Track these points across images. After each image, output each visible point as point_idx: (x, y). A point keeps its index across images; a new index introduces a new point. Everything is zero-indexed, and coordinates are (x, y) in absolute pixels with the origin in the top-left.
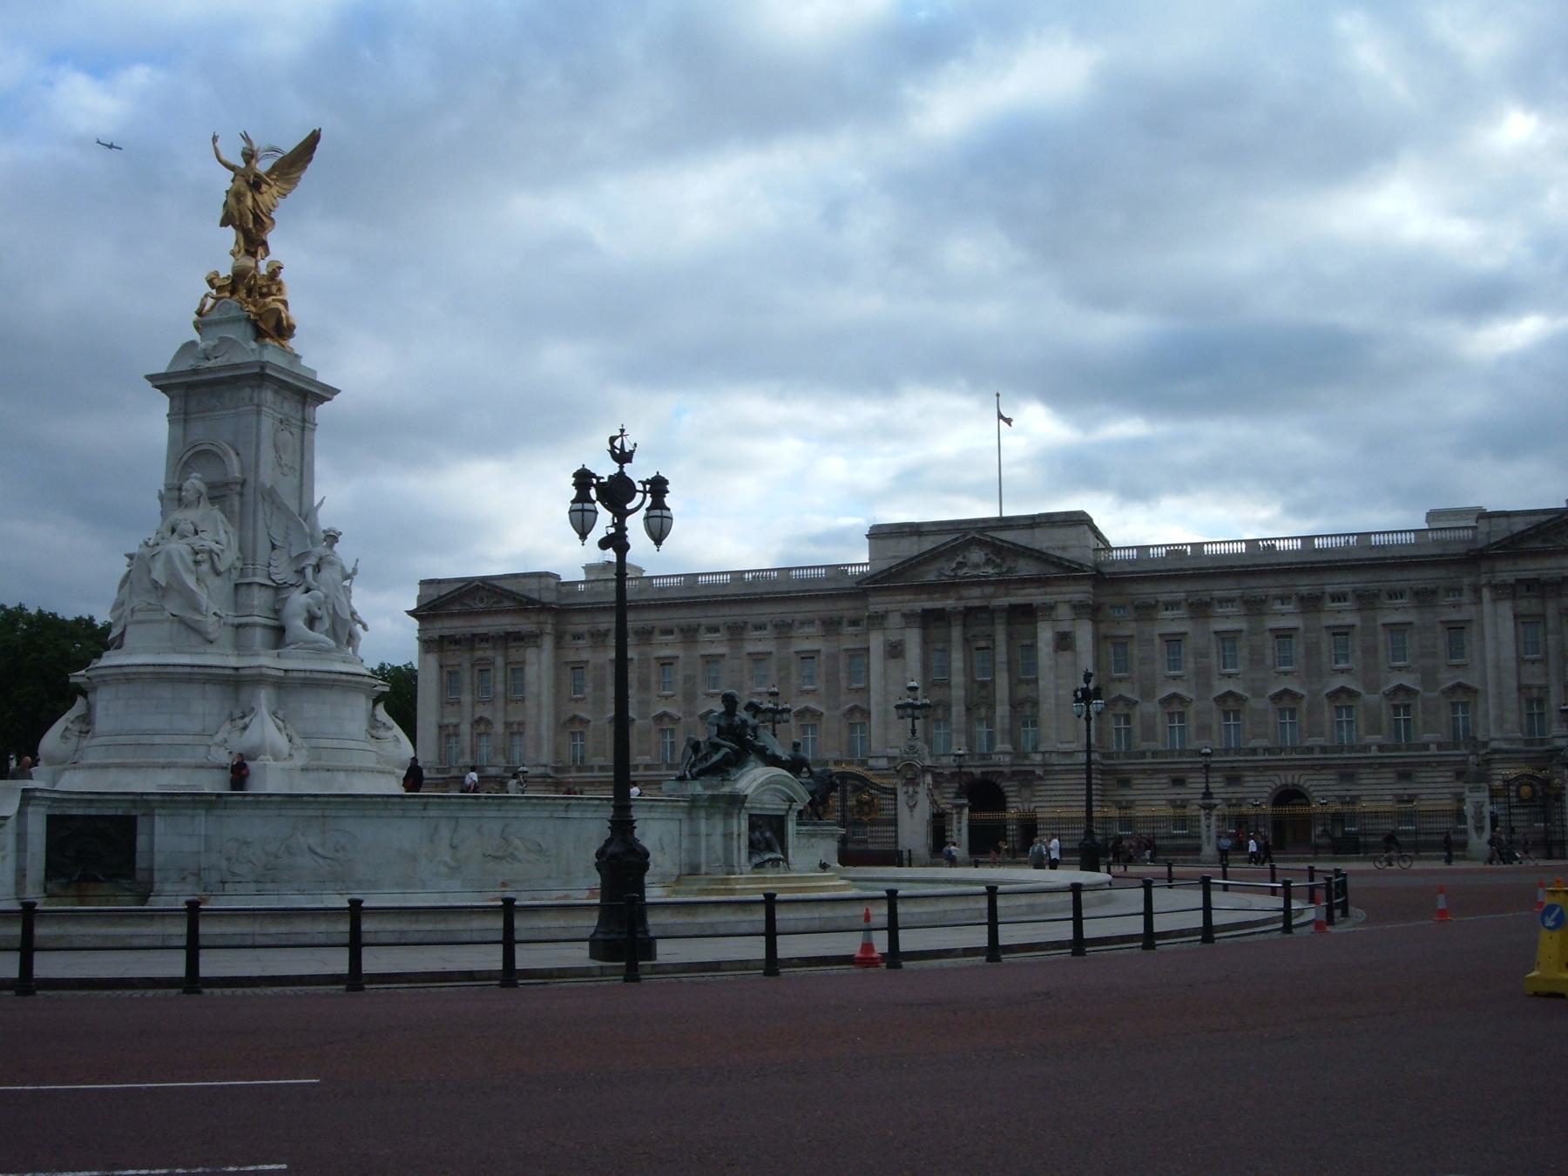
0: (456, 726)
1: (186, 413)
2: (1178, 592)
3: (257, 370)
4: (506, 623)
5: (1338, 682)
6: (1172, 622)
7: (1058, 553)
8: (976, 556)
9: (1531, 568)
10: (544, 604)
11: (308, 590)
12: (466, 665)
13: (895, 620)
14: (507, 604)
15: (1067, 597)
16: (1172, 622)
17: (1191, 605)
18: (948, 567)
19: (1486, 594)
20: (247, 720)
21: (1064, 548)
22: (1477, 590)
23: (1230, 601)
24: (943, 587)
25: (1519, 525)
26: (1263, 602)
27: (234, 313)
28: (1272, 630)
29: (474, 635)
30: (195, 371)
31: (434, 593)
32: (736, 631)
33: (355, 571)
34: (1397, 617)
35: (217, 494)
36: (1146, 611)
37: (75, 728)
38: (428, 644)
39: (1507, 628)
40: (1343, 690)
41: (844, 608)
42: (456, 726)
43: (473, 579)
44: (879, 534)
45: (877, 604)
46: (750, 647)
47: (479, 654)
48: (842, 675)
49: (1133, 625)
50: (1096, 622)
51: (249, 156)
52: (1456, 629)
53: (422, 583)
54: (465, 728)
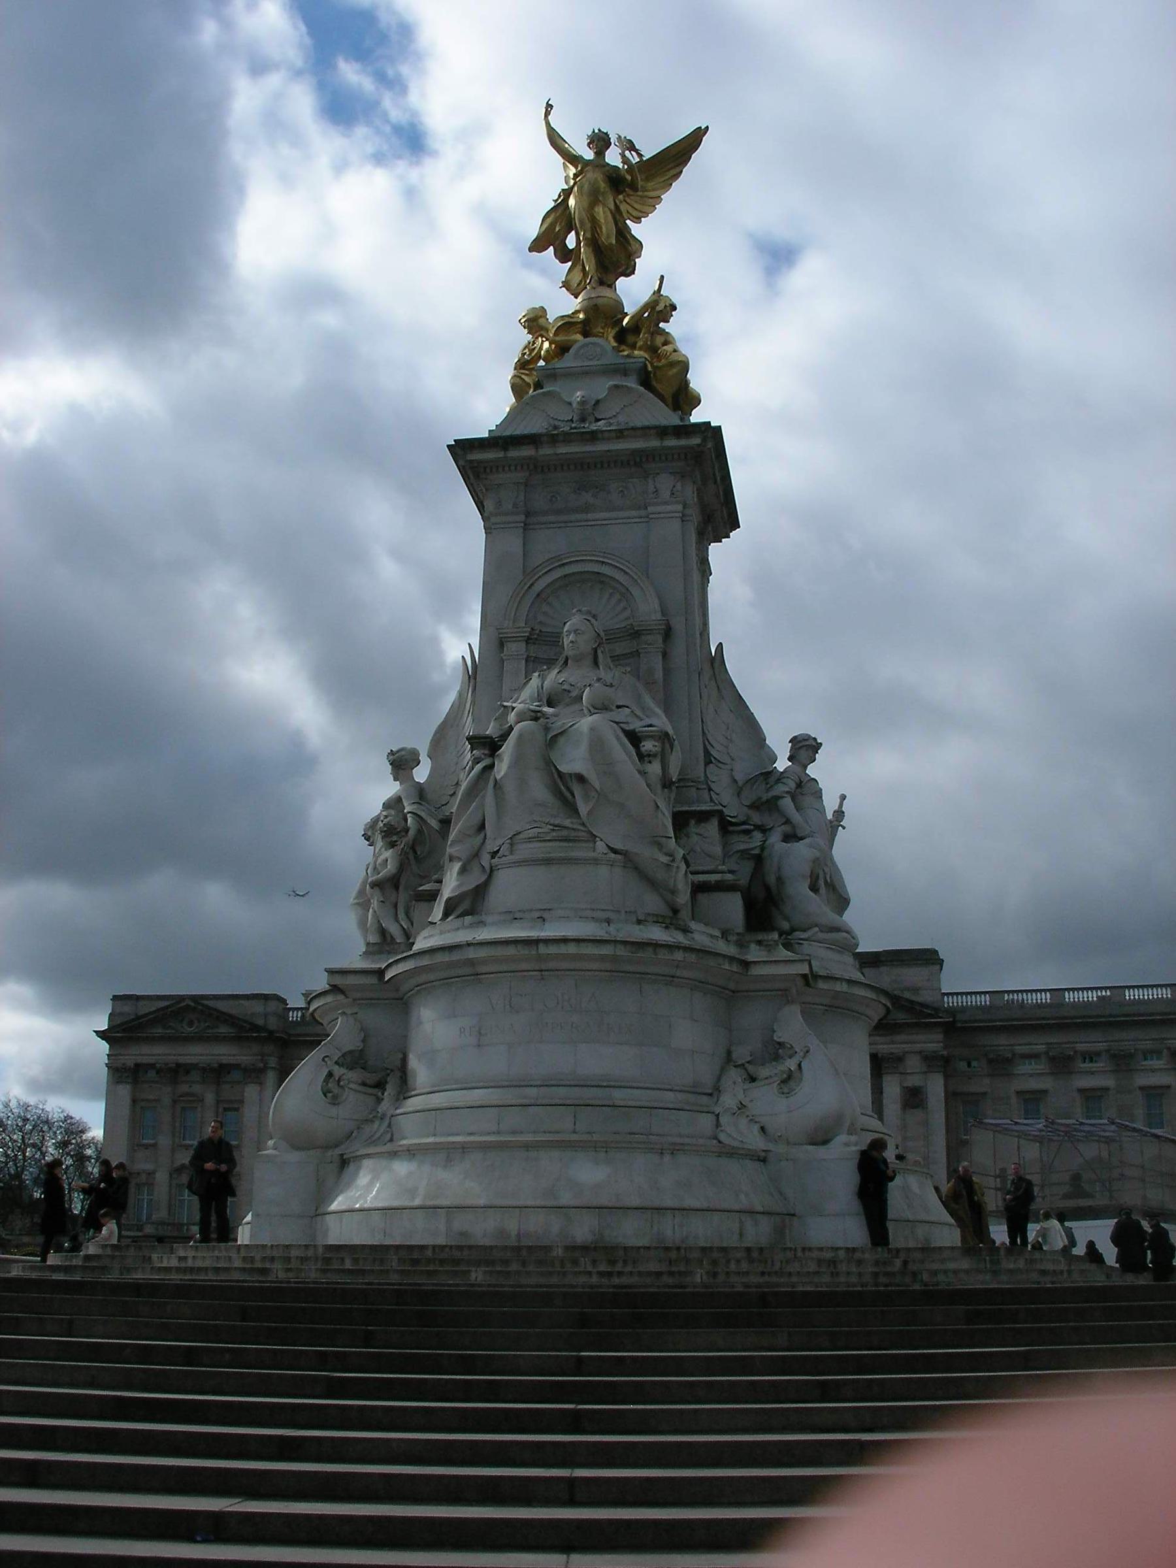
0: (151, 1174)
1: (528, 514)
2: (1038, 1043)
3: (696, 441)
4: (224, 1053)
6: (1031, 1076)
7: (907, 995)
10: (271, 1032)
11: (791, 837)
12: (167, 1100)
14: (223, 1030)
15: (918, 1047)
16: (1031, 1076)
17: (1053, 1059)
20: (792, 1064)
21: (916, 990)
23: (1098, 1054)
26: (1131, 1056)
27: (610, 359)
28: (1141, 1088)
29: (178, 1065)
30: (567, 438)
33: (839, 814)
35: (623, 646)
36: (1001, 1065)
37: (353, 1076)
38: (119, 1072)
42: (151, 1174)
43: (182, 998)
47: (184, 1088)
49: (987, 1081)
50: (947, 1077)
51: (600, 141)
53: (115, 998)
54: (162, 1177)
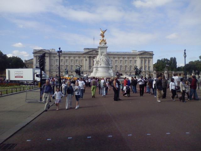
2: (112, 56)
5: (125, 65)
8: (94, 52)
9: (142, 56)
13: (87, 57)
18: (91, 53)
19: (138, 58)
22: (137, 58)
24: (91, 54)
25: (142, 52)
31: (35, 51)
32: (70, 57)
34: (131, 59)
38: (34, 56)
39: (140, 61)
40: (126, 66)
41: (81, 56)
44: (85, 49)
45: (84, 56)
46: (71, 59)
48: (80, 62)
52: (135, 61)
